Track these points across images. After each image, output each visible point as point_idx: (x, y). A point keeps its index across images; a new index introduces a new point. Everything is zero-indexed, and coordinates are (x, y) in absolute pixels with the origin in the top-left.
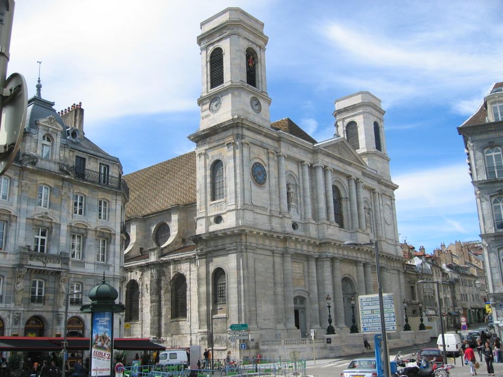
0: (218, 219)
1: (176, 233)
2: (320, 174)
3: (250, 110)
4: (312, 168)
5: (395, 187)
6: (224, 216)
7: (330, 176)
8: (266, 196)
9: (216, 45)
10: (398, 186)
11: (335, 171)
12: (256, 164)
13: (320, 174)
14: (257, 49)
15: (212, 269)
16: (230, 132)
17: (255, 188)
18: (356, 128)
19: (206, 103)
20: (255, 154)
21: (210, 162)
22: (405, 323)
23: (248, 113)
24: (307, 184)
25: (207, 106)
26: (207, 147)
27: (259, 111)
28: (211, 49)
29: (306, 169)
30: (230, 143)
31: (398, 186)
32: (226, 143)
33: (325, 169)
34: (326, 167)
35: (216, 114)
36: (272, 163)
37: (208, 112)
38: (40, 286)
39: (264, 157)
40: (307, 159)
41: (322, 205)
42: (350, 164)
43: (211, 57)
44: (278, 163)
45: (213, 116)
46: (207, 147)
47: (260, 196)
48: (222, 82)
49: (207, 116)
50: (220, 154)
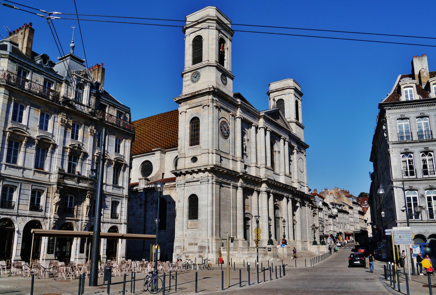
0: (194, 159)
1: (159, 168)
3: (221, 83)
10: (309, 146)
12: (223, 121)
15: (188, 195)
16: (206, 97)
19: (188, 76)
20: (222, 115)
22: (314, 240)
23: (219, 85)
25: (189, 78)
26: (188, 107)
27: (225, 84)
30: (206, 105)
31: (309, 146)
32: (203, 105)
34: (267, 128)
35: (196, 84)
37: (190, 82)
38: (71, 198)
45: (193, 85)
48: (201, 61)
49: (189, 85)
50: (198, 113)
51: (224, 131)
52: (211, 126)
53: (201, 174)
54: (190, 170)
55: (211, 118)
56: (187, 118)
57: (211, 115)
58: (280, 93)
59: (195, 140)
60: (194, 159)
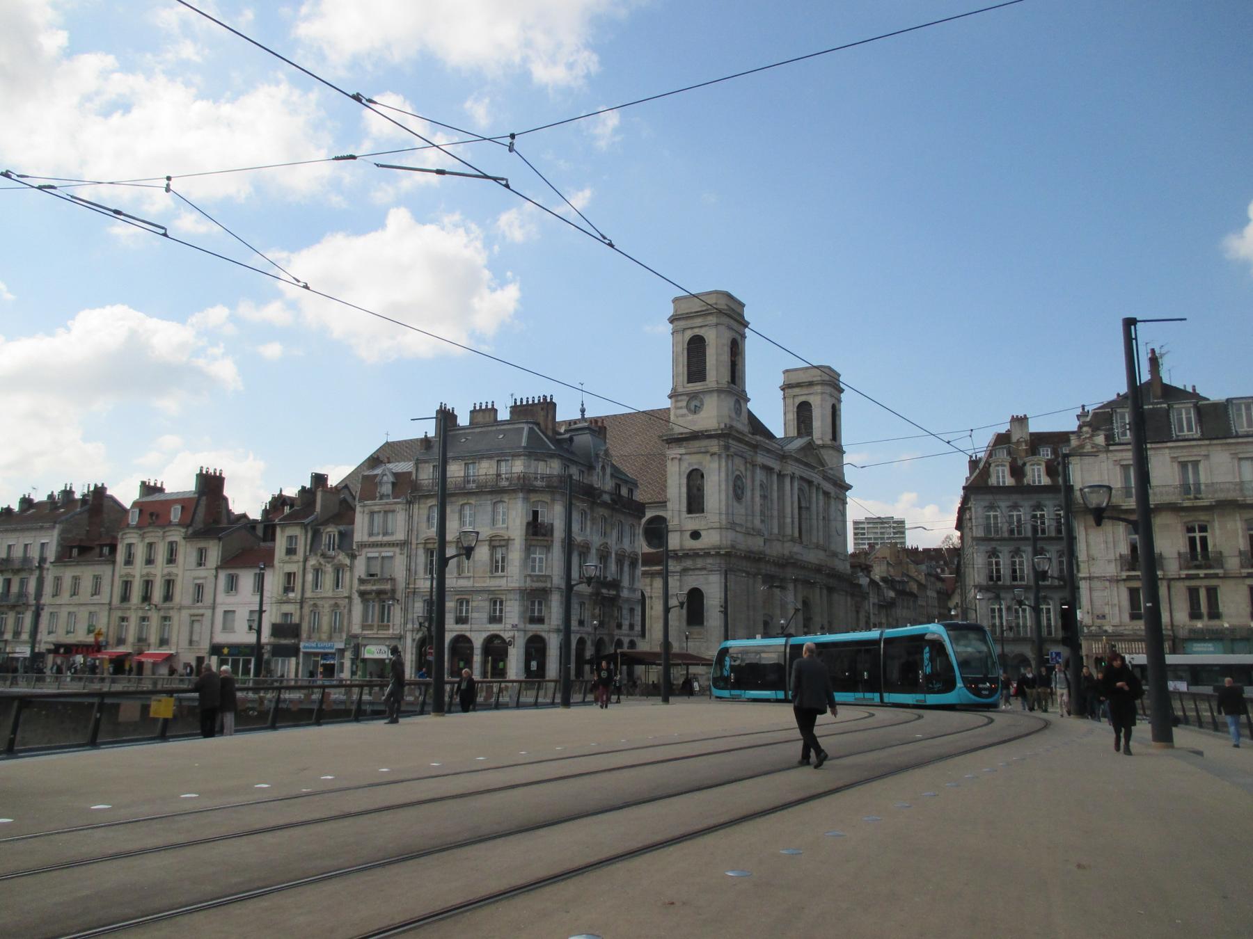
0: (695, 535)
2: (788, 481)
4: (781, 476)
5: (849, 487)
6: (703, 533)
7: (796, 484)
8: (743, 511)
9: (697, 332)
11: (802, 478)
13: (788, 481)
14: (739, 338)
16: (715, 442)
17: (735, 503)
18: (811, 411)
21: (686, 468)
24: (775, 495)
25: (684, 404)
28: (689, 335)
29: (775, 477)
33: (792, 478)
36: (749, 474)
37: (684, 411)
39: (742, 468)
40: (776, 465)
41: (789, 520)
42: (813, 468)
43: (689, 343)
44: (753, 473)
45: (691, 417)
46: (683, 451)
47: (740, 510)
49: (683, 416)
50: (700, 463)
51: (738, 491)
52: (723, 487)
53: (710, 561)
54: (691, 553)
55: (723, 475)
56: (683, 468)
57: (723, 469)
58: (805, 391)
59: (695, 503)
60: (695, 535)
